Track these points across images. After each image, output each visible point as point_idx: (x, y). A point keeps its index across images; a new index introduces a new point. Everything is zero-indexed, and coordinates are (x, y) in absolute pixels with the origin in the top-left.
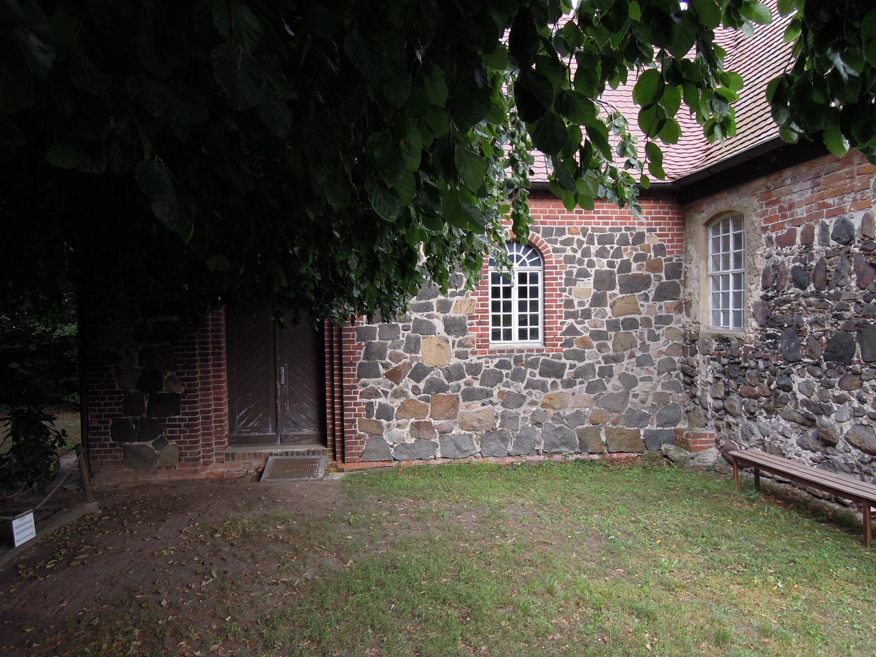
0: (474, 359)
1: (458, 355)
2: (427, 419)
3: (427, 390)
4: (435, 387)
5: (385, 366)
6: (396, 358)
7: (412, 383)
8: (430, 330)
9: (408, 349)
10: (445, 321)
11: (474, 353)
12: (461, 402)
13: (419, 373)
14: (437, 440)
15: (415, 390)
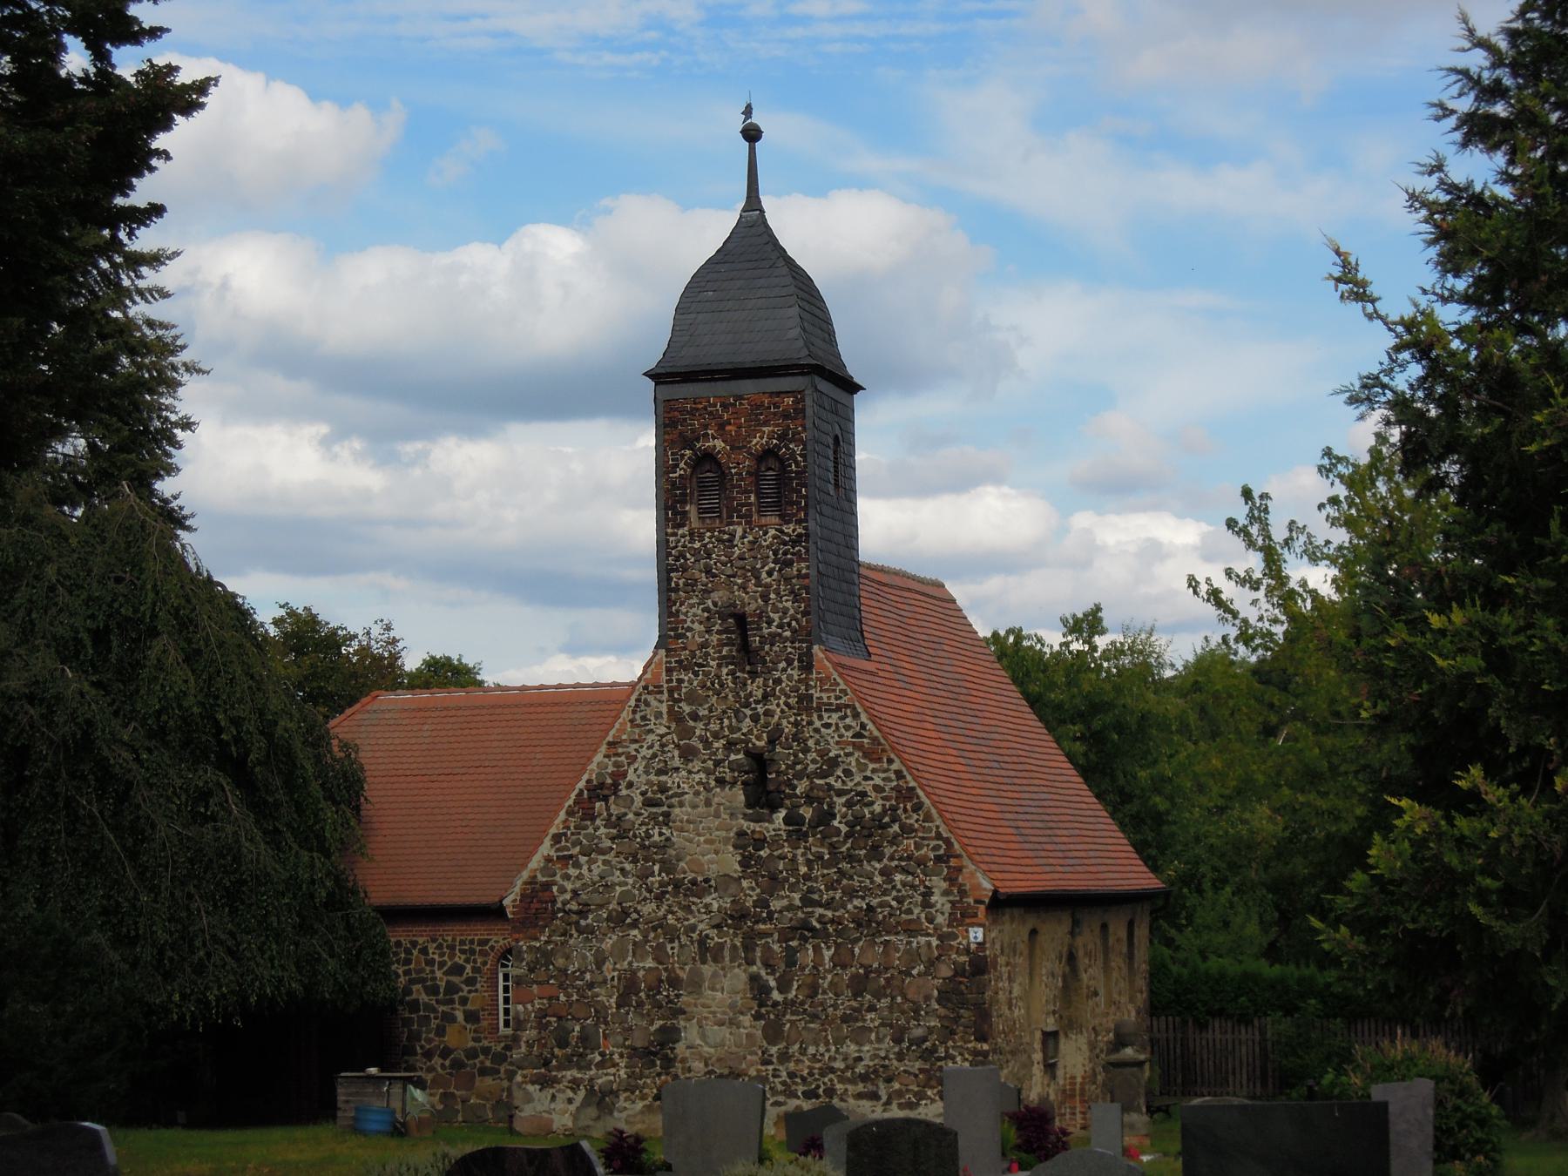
0: (485, 1043)
1: (475, 1040)
2: (452, 1090)
3: (452, 1066)
4: (457, 1065)
5: (422, 1047)
6: (429, 1041)
7: (440, 1061)
8: (453, 1019)
9: (437, 1034)
10: (465, 1012)
11: (486, 1038)
12: (478, 1079)
13: (446, 1053)
14: (459, 1107)
15: (443, 1066)
